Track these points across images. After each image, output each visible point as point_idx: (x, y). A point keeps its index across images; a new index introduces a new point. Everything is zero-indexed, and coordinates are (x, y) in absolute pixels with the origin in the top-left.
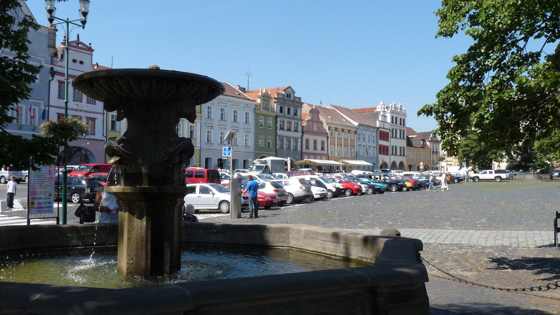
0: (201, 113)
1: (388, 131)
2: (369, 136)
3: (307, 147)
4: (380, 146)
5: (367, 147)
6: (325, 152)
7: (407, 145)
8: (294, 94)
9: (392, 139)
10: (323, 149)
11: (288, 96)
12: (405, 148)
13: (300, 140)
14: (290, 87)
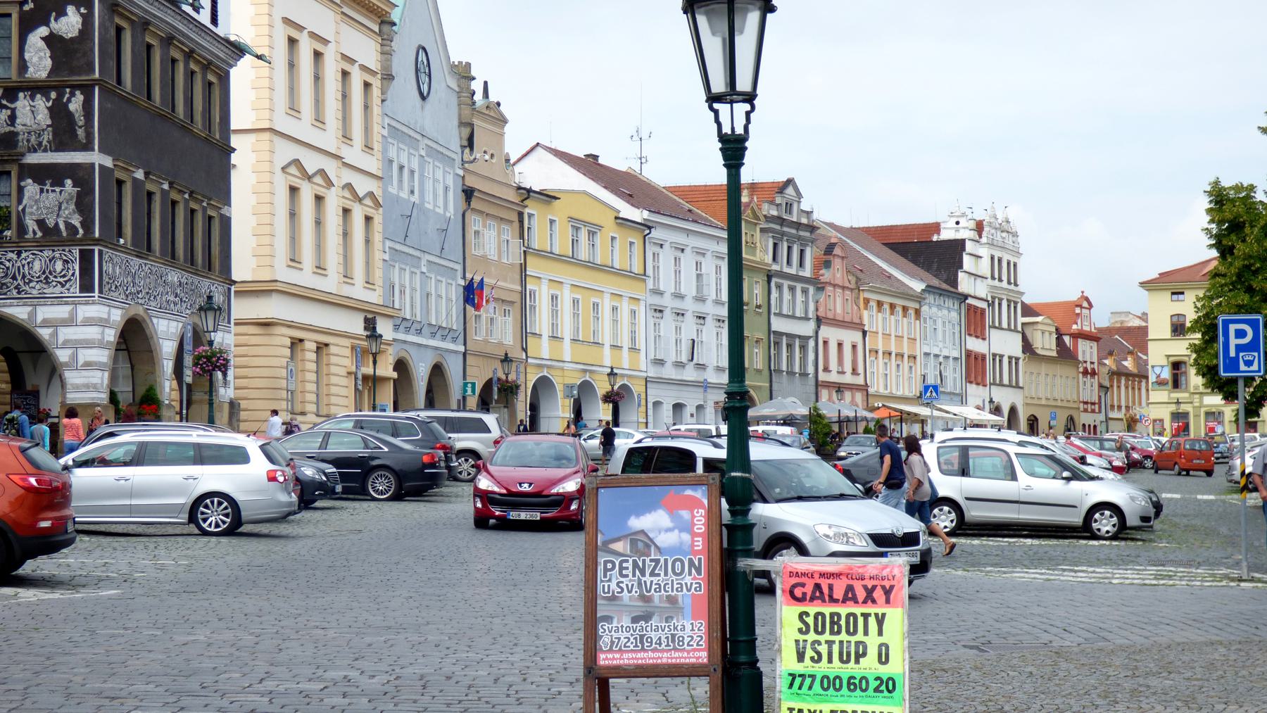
0: (645, 275)
1: (983, 305)
2: (944, 323)
3: (826, 369)
4: (969, 354)
5: (941, 359)
6: (859, 380)
7: (1024, 352)
8: (799, 202)
9: (992, 331)
10: (854, 372)
11: (789, 207)
12: (1017, 359)
13: (812, 343)
14: (790, 182)
